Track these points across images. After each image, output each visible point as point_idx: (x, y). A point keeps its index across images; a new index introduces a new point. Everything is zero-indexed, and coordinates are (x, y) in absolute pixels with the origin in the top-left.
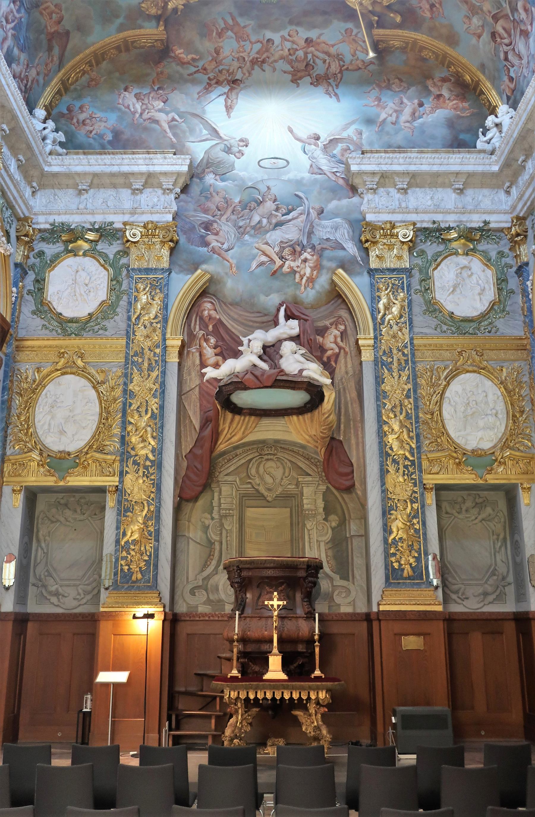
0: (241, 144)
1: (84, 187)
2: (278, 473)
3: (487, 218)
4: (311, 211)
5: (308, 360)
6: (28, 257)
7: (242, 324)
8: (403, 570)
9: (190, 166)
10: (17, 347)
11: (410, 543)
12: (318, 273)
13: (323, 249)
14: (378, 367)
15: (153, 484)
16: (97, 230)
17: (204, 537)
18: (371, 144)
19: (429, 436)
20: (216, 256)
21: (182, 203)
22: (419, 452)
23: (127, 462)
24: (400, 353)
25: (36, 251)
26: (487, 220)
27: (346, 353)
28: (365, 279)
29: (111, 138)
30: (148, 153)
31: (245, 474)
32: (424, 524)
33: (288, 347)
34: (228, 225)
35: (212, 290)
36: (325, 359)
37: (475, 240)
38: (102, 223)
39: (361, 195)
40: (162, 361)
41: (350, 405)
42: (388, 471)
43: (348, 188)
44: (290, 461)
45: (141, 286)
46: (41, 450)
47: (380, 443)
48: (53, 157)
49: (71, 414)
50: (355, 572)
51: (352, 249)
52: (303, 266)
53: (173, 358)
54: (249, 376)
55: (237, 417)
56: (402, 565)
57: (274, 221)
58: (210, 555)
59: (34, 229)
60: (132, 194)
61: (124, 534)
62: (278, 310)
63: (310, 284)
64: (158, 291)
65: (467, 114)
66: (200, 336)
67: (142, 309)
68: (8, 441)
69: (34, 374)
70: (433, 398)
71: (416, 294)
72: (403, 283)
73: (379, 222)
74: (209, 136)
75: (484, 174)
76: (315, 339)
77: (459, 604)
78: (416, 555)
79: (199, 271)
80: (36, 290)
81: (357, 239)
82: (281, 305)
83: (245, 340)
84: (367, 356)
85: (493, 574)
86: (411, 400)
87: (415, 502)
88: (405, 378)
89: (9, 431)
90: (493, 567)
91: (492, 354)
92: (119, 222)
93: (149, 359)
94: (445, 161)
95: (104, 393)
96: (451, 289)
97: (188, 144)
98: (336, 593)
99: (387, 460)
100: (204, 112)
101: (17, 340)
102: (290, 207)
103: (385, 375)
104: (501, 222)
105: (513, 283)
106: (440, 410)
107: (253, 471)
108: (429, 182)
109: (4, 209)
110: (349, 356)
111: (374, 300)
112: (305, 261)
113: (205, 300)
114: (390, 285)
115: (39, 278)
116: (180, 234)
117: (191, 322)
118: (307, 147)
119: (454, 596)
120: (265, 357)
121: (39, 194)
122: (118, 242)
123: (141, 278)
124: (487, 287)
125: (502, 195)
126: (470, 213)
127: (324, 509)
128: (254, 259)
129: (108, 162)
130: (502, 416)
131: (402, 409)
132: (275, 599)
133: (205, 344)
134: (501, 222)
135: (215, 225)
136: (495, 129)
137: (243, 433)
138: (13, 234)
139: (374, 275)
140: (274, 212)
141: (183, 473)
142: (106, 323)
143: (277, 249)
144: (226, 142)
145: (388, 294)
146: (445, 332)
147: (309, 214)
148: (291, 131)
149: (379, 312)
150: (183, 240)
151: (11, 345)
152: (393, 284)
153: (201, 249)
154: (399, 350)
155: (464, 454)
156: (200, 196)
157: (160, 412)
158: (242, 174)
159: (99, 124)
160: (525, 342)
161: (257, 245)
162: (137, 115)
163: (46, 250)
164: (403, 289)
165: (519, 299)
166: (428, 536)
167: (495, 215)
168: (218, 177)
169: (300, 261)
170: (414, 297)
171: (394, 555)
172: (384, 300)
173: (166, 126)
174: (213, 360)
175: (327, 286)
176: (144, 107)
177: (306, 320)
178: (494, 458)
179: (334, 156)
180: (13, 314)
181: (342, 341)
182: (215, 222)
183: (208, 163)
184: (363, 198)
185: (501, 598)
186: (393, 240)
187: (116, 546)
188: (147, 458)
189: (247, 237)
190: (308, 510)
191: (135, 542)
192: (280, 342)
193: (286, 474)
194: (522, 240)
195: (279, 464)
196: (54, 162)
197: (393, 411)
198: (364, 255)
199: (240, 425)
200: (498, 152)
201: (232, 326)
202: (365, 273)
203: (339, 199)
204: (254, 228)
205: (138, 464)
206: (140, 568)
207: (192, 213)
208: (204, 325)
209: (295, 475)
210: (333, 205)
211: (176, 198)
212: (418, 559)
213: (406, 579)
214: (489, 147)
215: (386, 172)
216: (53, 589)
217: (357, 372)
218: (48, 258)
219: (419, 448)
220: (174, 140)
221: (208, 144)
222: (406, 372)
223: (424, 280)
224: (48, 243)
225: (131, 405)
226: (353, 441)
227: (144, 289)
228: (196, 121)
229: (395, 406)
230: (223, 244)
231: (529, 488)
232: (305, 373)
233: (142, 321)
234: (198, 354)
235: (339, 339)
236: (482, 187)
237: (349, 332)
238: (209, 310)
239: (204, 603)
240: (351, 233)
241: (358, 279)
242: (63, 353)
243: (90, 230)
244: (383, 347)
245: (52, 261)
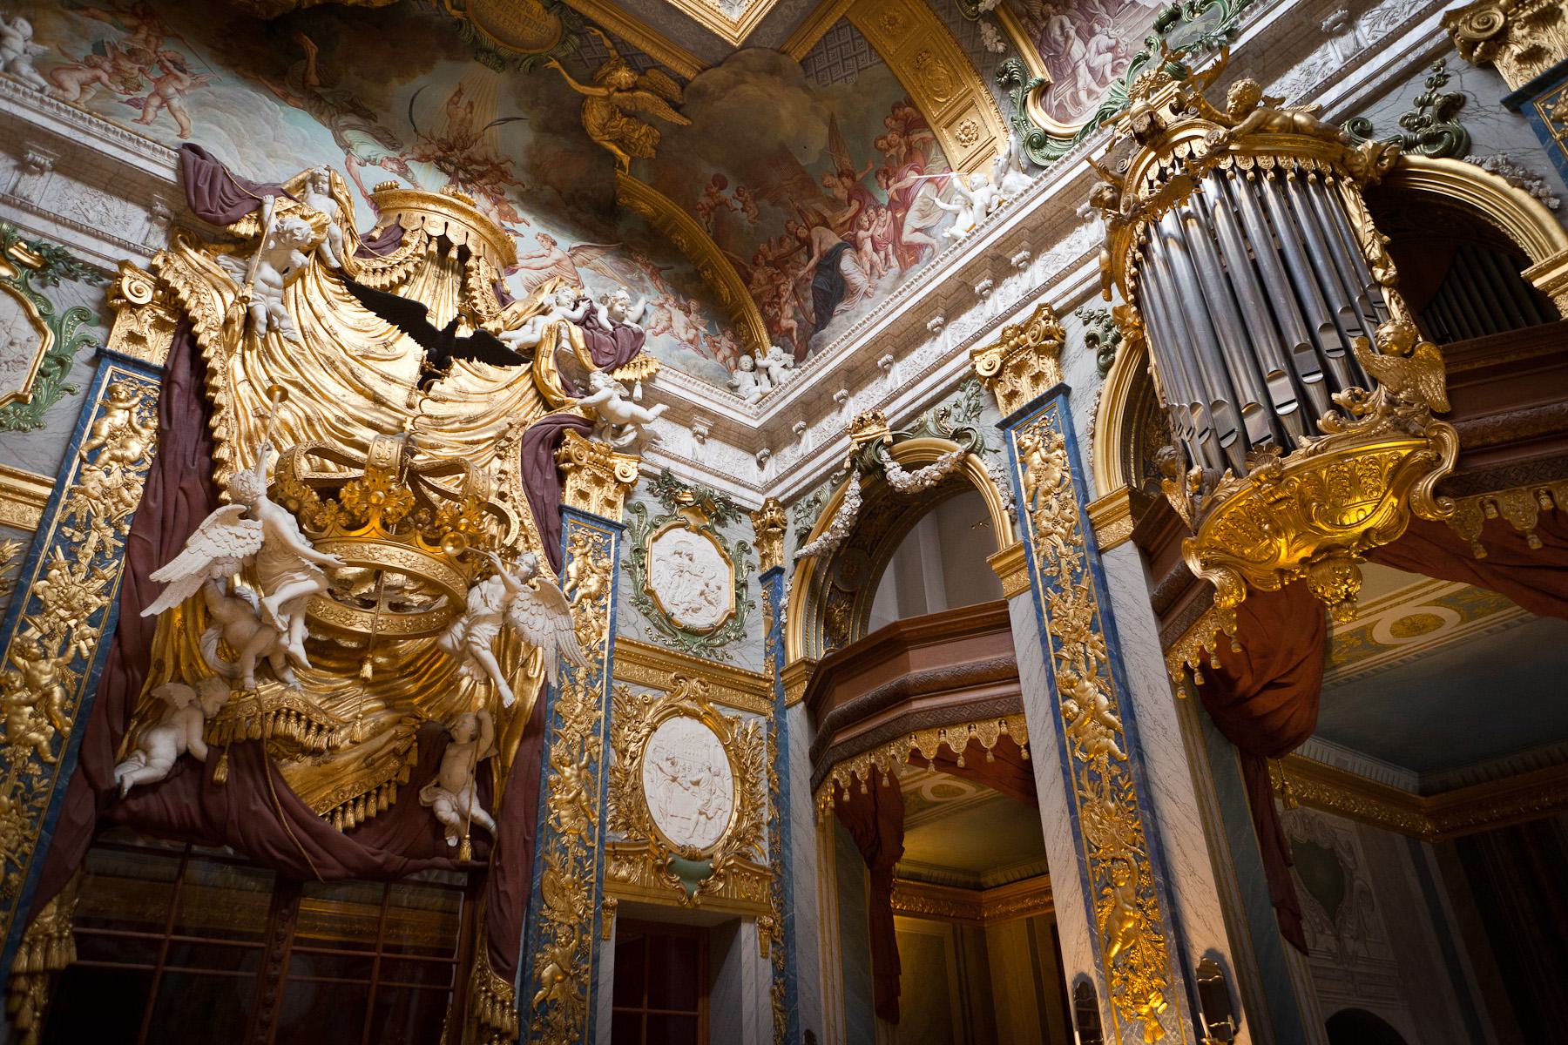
67: (112, 436)
93: (101, 542)
125: (752, 462)
131: (582, 752)
145: (586, 554)
149: (569, 579)
188: (37, 756)
219: (602, 824)
225: (25, 627)
233: (105, 456)
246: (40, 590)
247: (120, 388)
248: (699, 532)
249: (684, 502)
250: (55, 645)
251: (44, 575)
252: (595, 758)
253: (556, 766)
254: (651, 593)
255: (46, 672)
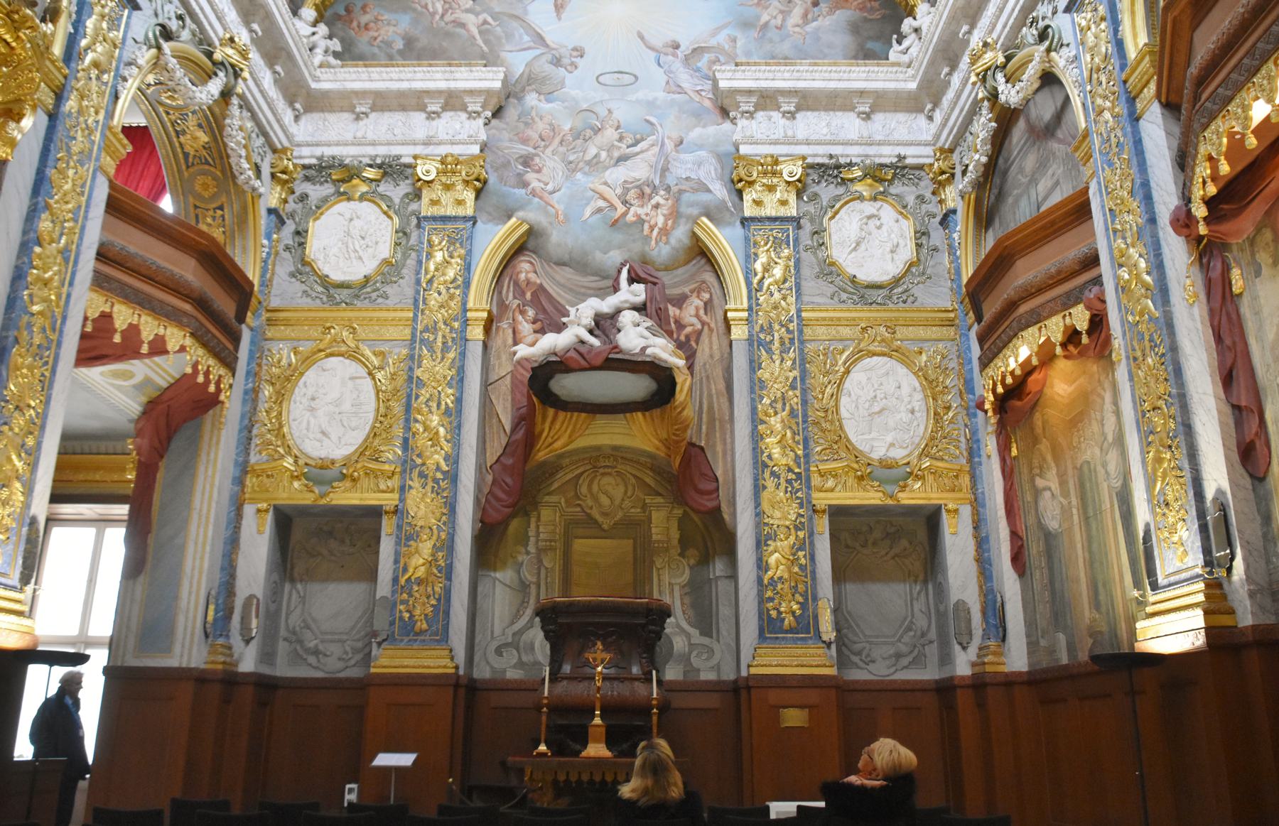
0: (575, 53)
1: (364, 110)
2: (618, 492)
3: (903, 151)
4: (666, 140)
5: (654, 335)
6: (285, 201)
7: (571, 290)
8: (783, 620)
9: (505, 81)
10: (268, 320)
11: (793, 584)
12: (674, 222)
13: (681, 192)
14: (753, 346)
15: (445, 503)
16: (380, 166)
17: (515, 576)
18: (748, 53)
19: (821, 441)
20: (536, 200)
21: (494, 131)
22: (807, 463)
23: (411, 473)
24: (783, 330)
25: (297, 194)
26: (903, 154)
27: (711, 330)
28: (738, 231)
29: (401, 47)
30: (450, 65)
31: (572, 494)
32: (813, 558)
33: (628, 317)
34: (555, 161)
35: (531, 244)
36: (682, 338)
37: (886, 180)
38: (385, 157)
39: (733, 121)
40: (461, 339)
41: (715, 400)
42: (765, 487)
43: (717, 112)
44: (635, 476)
45: (436, 240)
46: (296, 457)
47: (754, 449)
48: (323, 70)
49: (337, 410)
50: (721, 625)
51: (720, 191)
52: (653, 213)
53: (476, 332)
54: (572, 354)
55: (562, 415)
56: (781, 613)
57: (616, 154)
58: (523, 602)
59: (295, 165)
60: (428, 118)
61: (405, 570)
62: (619, 272)
63: (664, 238)
64: (458, 245)
65: (877, 15)
66: (514, 306)
67: (437, 269)
68: (253, 446)
69: (290, 356)
70: (828, 390)
71: (806, 250)
72: (788, 236)
73: (756, 155)
74: (532, 44)
75: (897, 93)
76: (667, 310)
77: (862, 669)
78: (801, 599)
79: (513, 220)
80: (296, 245)
81: (727, 178)
82: (623, 265)
83: (572, 311)
84: (739, 332)
85: (909, 629)
86: (798, 392)
87: (800, 530)
88: (789, 363)
89: (255, 432)
90: (909, 619)
91: (911, 332)
92: (408, 156)
93: (444, 337)
94: (846, 76)
95: (383, 381)
96: (854, 245)
97: (503, 54)
98: (694, 653)
99: (763, 472)
100: (526, 12)
101: (268, 311)
102: (638, 136)
103: (763, 358)
104: (920, 157)
105: (937, 236)
106: (837, 406)
107: (584, 490)
108: (824, 103)
109: (254, 135)
110: (715, 334)
111: (750, 258)
112: (657, 206)
113: (523, 258)
114: (771, 238)
115: (300, 229)
116: (490, 171)
117: (502, 287)
118: (663, 58)
119: (855, 659)
120: (597, 332)
121: (303, 120)
122: (407, 182)
123: (435, 229)
124: (902, 243)
125: (921, 120)
126: (879, 144)
127: (680, 541)
128: (587, 204)
129: (394, 76)
130: (921, 416)
131: (784, 404)
132: (599, 652)
133: (520, 318)
134: (920, 157)
135: (537, 160)
136: (913, 36)
137: (570, 437)
138: (266, 171)
139: (749, 226)
140: (616, 143)
141: (486, 490)
142: (389, 290)
143: (619, 191)
144: (554, 52)
145: (768, 250)
146: (844, 302)
147: (663, 145)
148: (641, 37)
149: (756, 274)
150: (492, 180)
151: (260, 315)
152: (775, 238)
153: (516, 191)
154: (782, 326)
155: (869, 464)
156: (518, 121)
157: (456, 407)
158: (575, 93)
159: (387, 28)
160: (952, 315)
161: (592, 186)
162: (437, 17)
163: (311, 193)
164: (788, 245)
165: (946, 259)
166: (817, 576)
167: (912, 147)
168: (542, 97)
169: (650, 207)
170: (804, 255)
171: (771, 599)
172: (763, 259)
173: (475, 31)
174: (531, 338)
175: (687, 241)
176: (447, 6)
177: (655, 284)
178: (908, 470)
179: (698, 70)
180: (263, 275)
181: (706, 314)
182: (537, 155)
183: (529, 79)
184: (735, 124)
185: (918, 661)
186: (775, 180)
187: (393, 586)
188: (438, 468)
189: (579, 176)
190: (658, 542)
191: (420, 582)
192: (618, 311)
193: (629, 493)
194: (947, 179)
195: (619, 480)
196: (323, 77)
197: (772, 407)
198: (736, 199)
199: (565, 425)
200: (915, 64)
201: (558, 293)
202: (738, 223)
203: (704, 127)
204: (589, 163)
205: (426, 477)
206: (426, 615)
207: (508, 144)
208: (519, 292)
209: (642, 496)
210: (696, 134)
211: (486, 124)
212: (803, 606)
213: (786, 632)
214: (905, 58)
215: (766, 89)
216: (312, 645)
217: (726, 355)
218: (315, 202)
219: (806, 456)
220: (485, 48)
221: (530, 55)
222: (792, 355)
223: (816, 232)
224: (314, 184)
225: (417, 397)
226: (719, 448)
227: (440, 243)
228: (515, 24)
229: (775, 401)
230: (546, 184)
231: (956, 511)
232: (649, 351)
233: (435, 285)
234: (510, 331)
235: (702, 312)
236: (895, 111)
237: (716, 301)
238: (527, 272)
239: (514, 667)
240: (720, 171)
241: (728, 231)
242: (329, 328)
243: (371, 166)
244: (760, 322)
245: (318, 208)
246: (419, 375)
247: (434, 238)
248: (874, 199)
249: (855, 178)
250: (434, 405)
251: (419, 367)
252: (795, 407)
253: (764, 418)
254: (833, 264)
255: (435, 420)
